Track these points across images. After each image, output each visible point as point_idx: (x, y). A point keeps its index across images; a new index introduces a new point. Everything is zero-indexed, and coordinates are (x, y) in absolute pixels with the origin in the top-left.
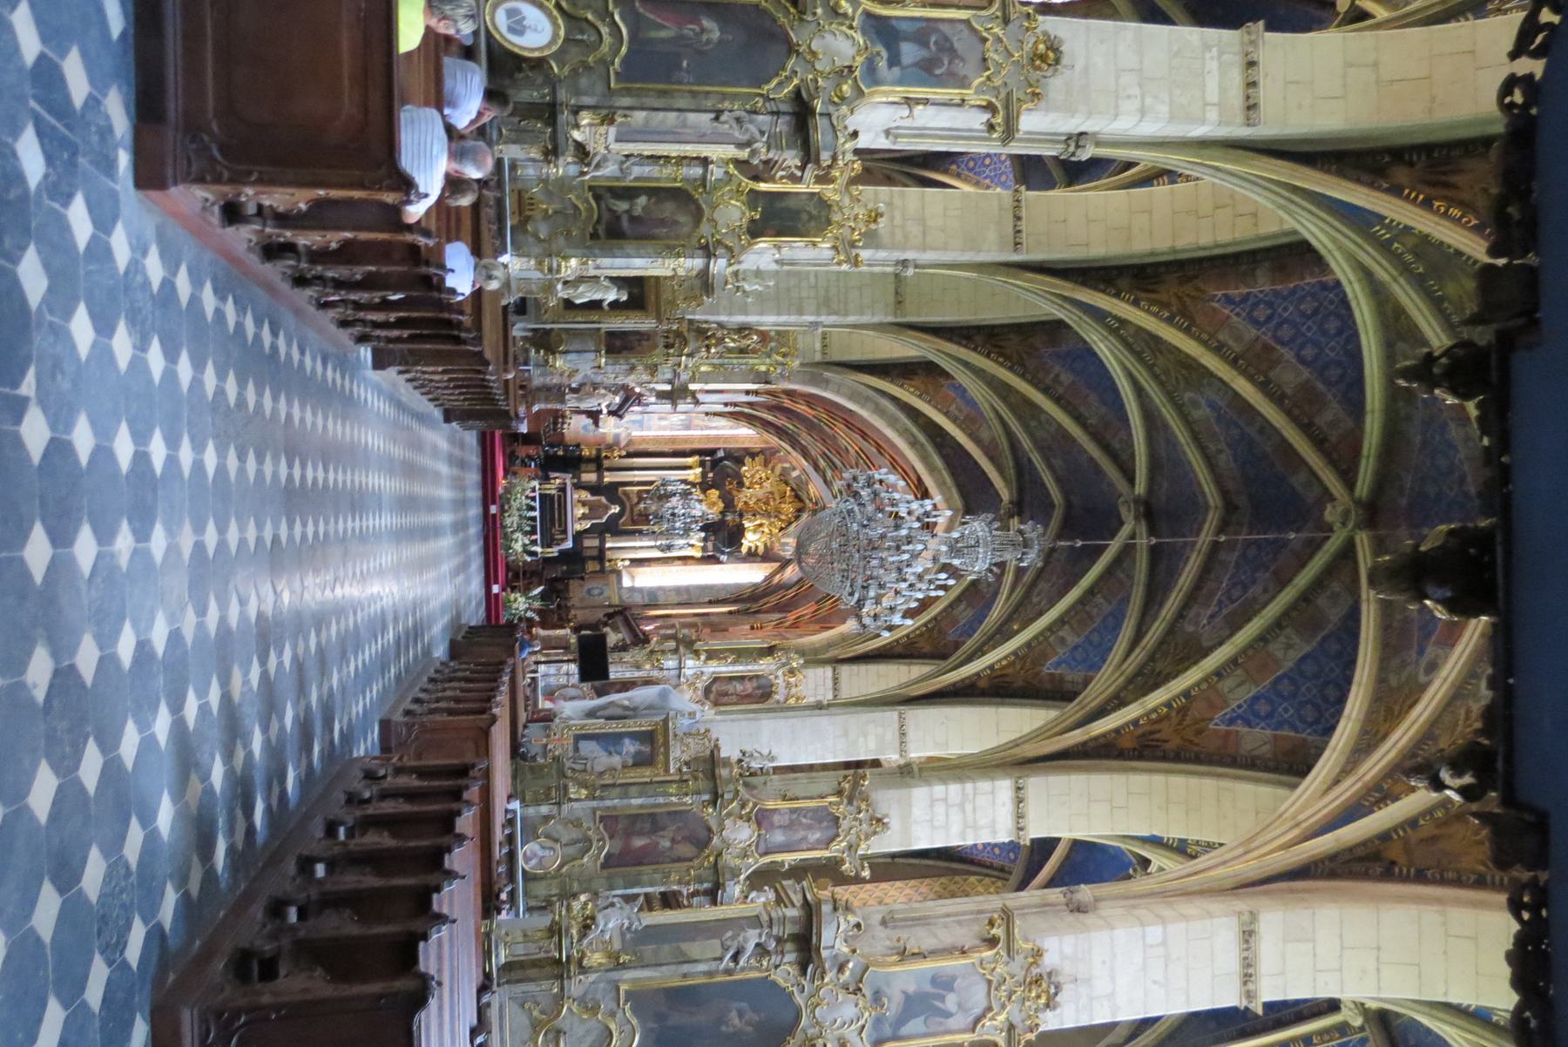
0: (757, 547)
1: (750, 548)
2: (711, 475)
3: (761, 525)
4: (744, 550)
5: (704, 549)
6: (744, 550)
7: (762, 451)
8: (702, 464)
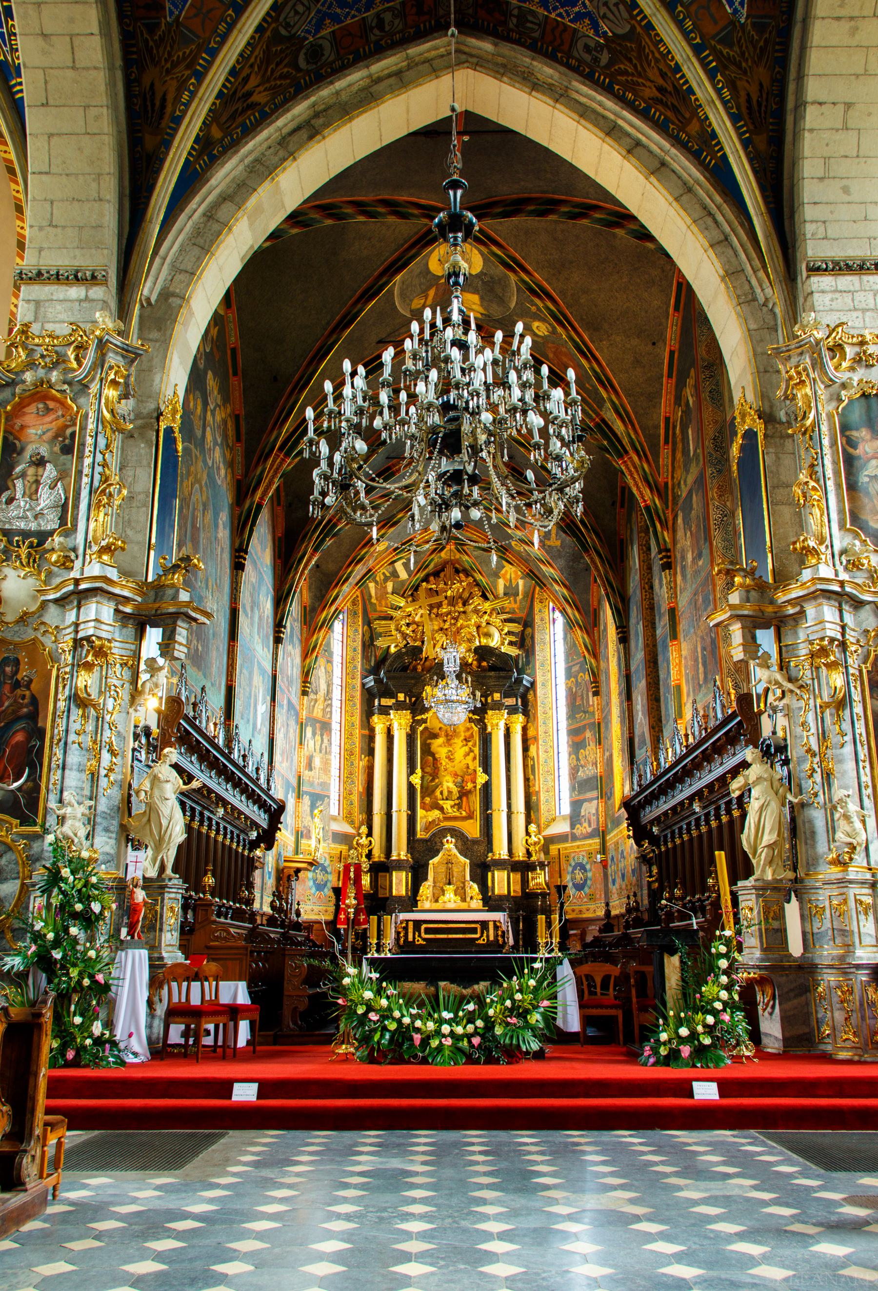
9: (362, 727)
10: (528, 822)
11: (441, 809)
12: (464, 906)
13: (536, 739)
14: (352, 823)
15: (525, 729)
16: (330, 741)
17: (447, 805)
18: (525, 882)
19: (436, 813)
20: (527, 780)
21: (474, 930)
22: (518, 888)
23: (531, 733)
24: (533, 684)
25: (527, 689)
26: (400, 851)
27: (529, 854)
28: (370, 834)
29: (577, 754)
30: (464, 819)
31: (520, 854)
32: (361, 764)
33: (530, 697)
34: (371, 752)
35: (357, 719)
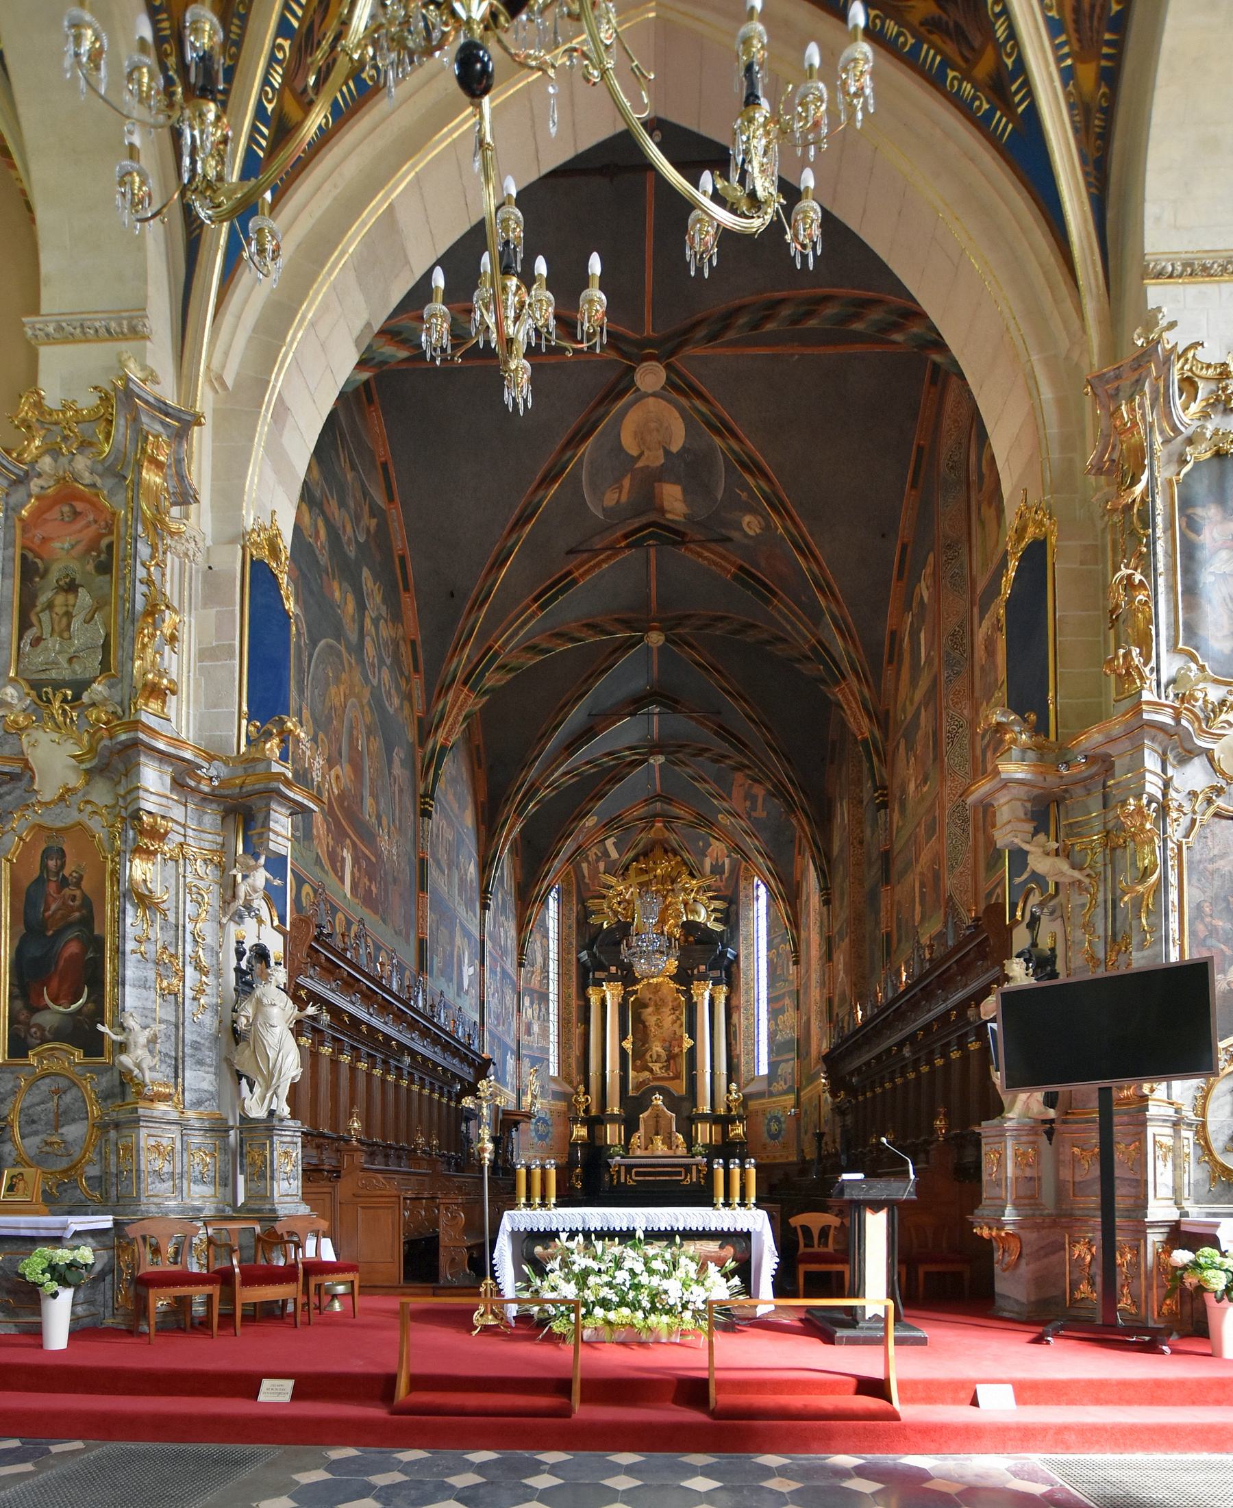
0: (714, 910)
1: (716, 920)
2: (613, 969)
3: (686, 904)
4: (718, 927)
5: (716, 982)
6: (718, 927)
7: (582, 901)
8: (598, 984)
9: (578, 998)
10: (729, 1081)
11: (651, 1071)
12: (670, 1153)
13: (738, 1007)
14: (570, 1083)
15: (728, 999)
16: (547, 1009)
17: (656, 1067)
18: (725, 1133)
19: (647, 1074)
20: (729, 1045)
21: (679, 1174)
22: (719, 1138)
23: (734, 1002)
24: (737, 957)
25: (731, 962)
26: (614, 1108)
27: (729, 1109)
28: (587, 1092)
29: (776, 1019)
30: (673, 1079)
31: (722, 1110)
32: (578, 1031)
33: (734, 969)
34: (586, 1021)
35: (573, 991)
